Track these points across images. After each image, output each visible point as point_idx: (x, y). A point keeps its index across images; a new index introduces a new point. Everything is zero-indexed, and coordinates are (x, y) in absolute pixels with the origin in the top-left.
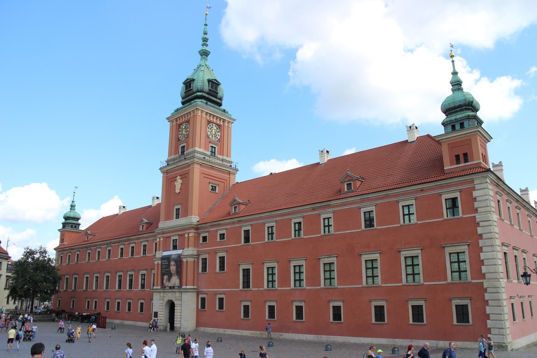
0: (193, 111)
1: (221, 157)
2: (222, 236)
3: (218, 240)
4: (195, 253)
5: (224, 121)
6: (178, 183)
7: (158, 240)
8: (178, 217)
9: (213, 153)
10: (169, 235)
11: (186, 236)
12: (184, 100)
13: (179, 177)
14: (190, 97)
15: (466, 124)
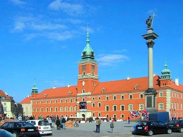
0: (88, 62)
1: (95, 75)
2: (99, 98)
3: (98, 99)
4: (91, 102)
5: (96, 64)
6: (84, 83)
7: (77, 98)
8: (84, 92)
9: (93, 74)
10: (81, 97)
11: (88, 98)
12: (82, 58)
13: (84, 82)
14: (85, 57)
15: (166, 77)
